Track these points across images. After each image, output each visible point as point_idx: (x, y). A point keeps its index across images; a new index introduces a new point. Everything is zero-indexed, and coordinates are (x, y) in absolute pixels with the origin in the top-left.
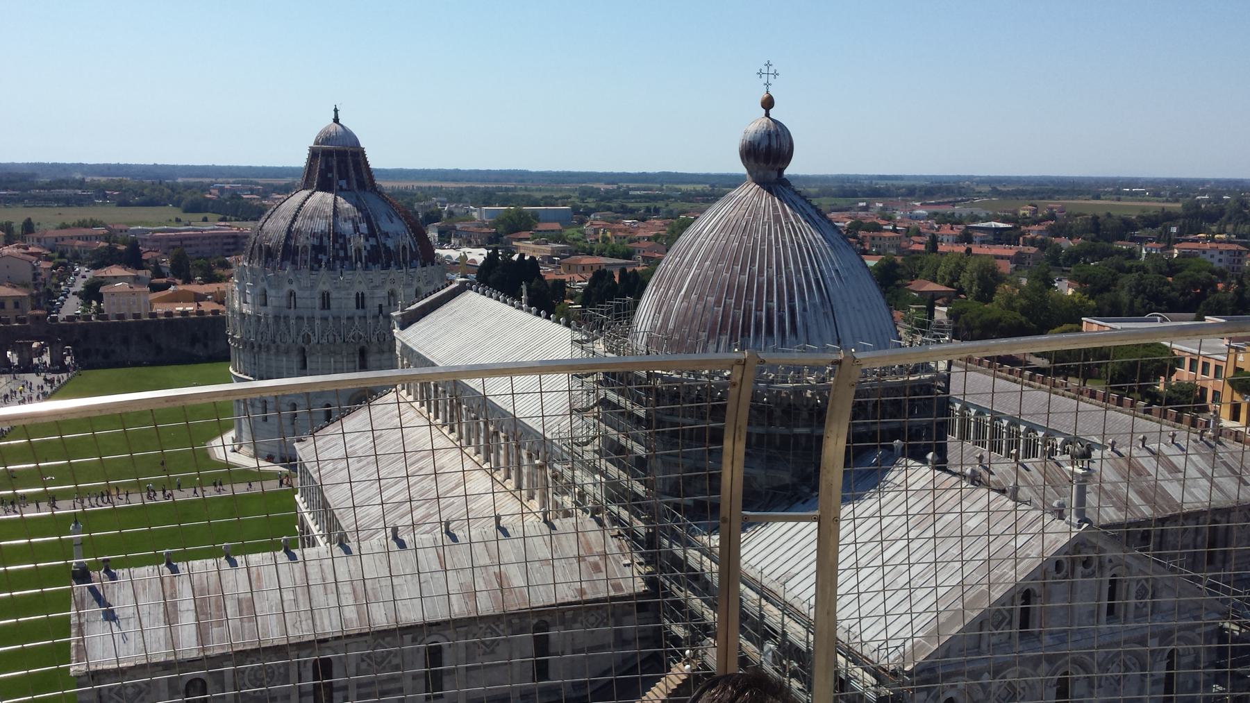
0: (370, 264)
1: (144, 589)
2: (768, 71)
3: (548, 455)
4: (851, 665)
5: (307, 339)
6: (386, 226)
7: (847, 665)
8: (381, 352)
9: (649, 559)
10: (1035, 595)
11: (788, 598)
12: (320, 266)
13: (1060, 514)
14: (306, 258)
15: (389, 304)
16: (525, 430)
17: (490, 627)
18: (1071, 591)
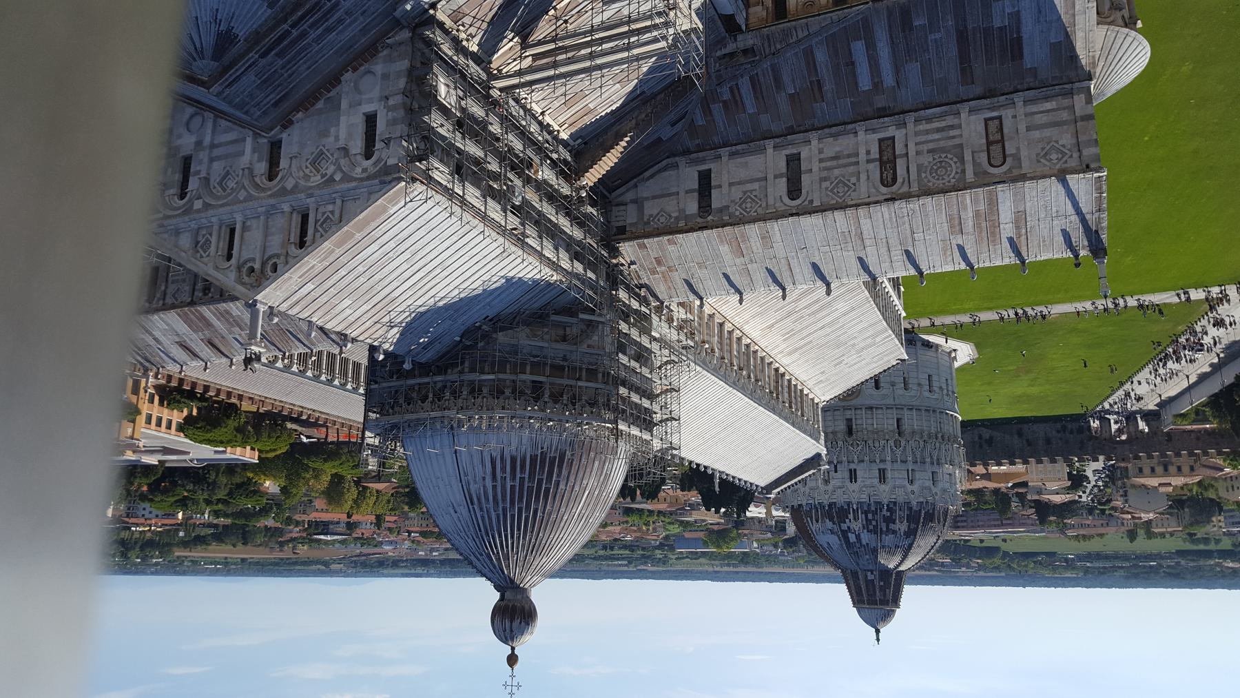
0: (846, 507)
1: (1044, 241)
2: (512, 687)
3: (698, 352)
4: (450, 186)
5: (897, 444)
6: (834, 540)
7: (453, 186)
8: (834, 433)
9: (616, 269)
10: (295, 244)
11: (501, 240)
12: (888, 505)
13: (271, 312)
14: (901, 513)
15: (828, 473)
16: (717, 372)
17: (748, 213)
18: (265, 248)
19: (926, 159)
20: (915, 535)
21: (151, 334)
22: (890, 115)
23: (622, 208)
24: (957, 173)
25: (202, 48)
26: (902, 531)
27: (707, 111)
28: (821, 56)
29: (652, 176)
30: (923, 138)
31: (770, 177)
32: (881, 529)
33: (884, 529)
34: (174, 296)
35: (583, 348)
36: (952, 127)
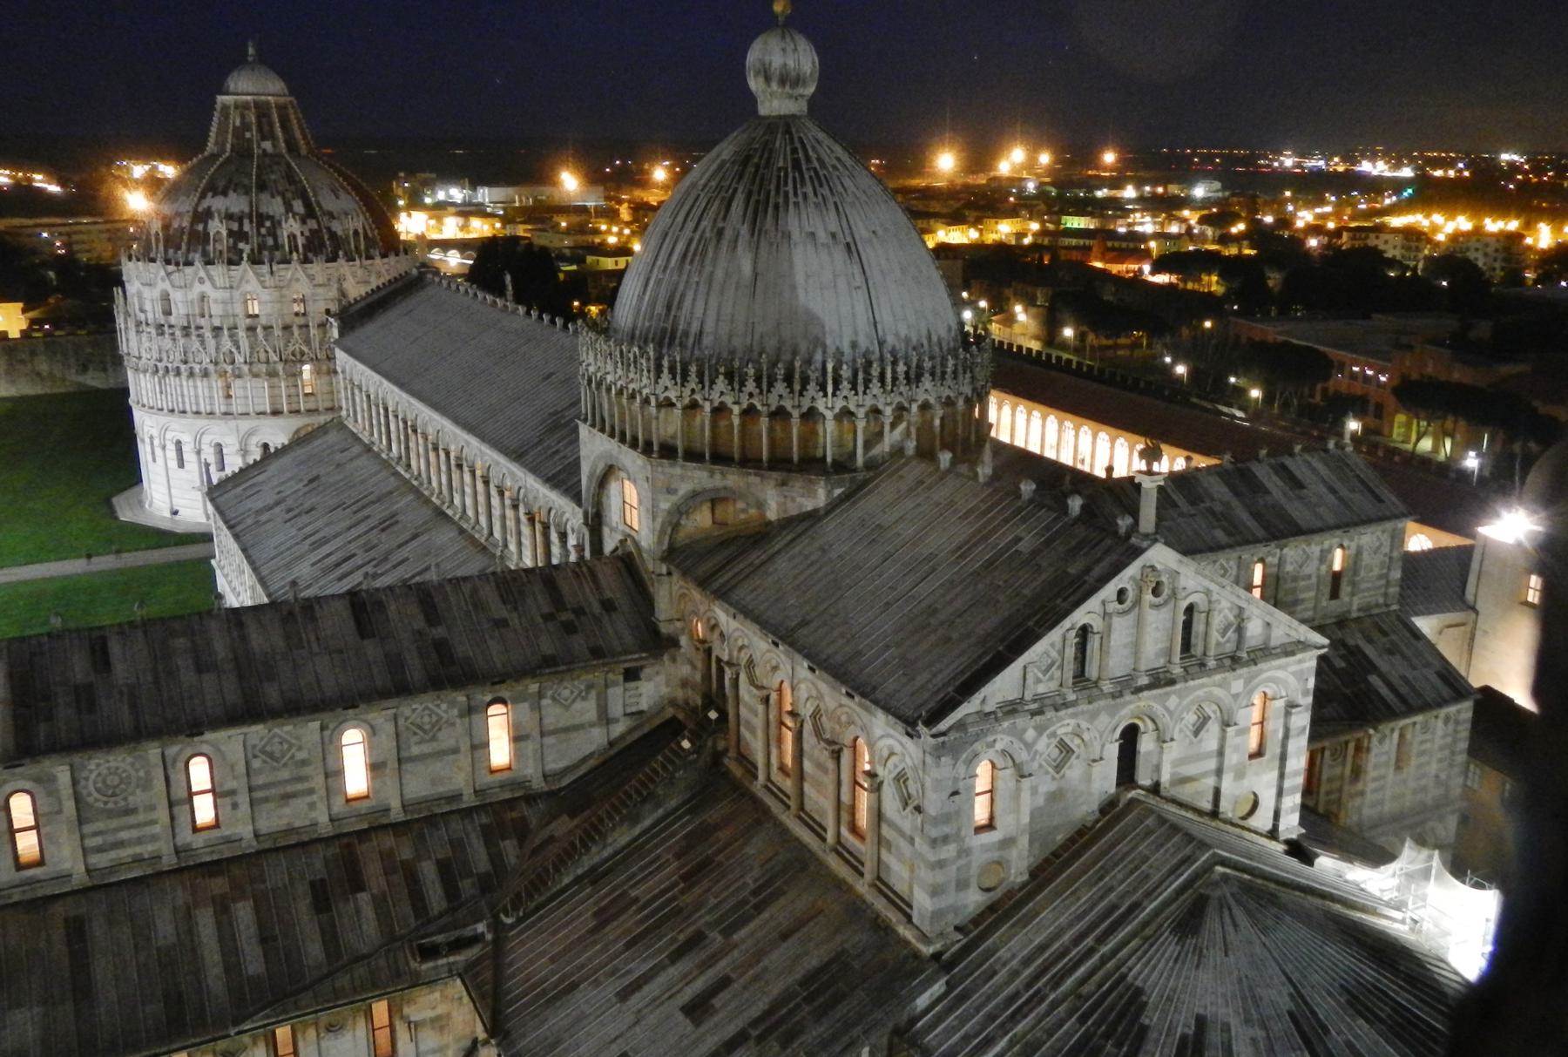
0: (310, 255)
12: (242, 259)
14: (219, 247)
17: (427, 708)
19: (137, 798)
20: (195, 211)
21: (1341, 499)
22: (202, 865)
23: (634, 709)
24: (87, 779)
25: (1222, 912)
26: (217, 219)
27: (496, 858)
28: (314, 951)
29: (584, 760)
30: (148, 830)
31: (393, 764)
32: (251, 222)
33: (246, 223)
34: (1308, 557)
35: (684, 489)
36: (100, 850)
